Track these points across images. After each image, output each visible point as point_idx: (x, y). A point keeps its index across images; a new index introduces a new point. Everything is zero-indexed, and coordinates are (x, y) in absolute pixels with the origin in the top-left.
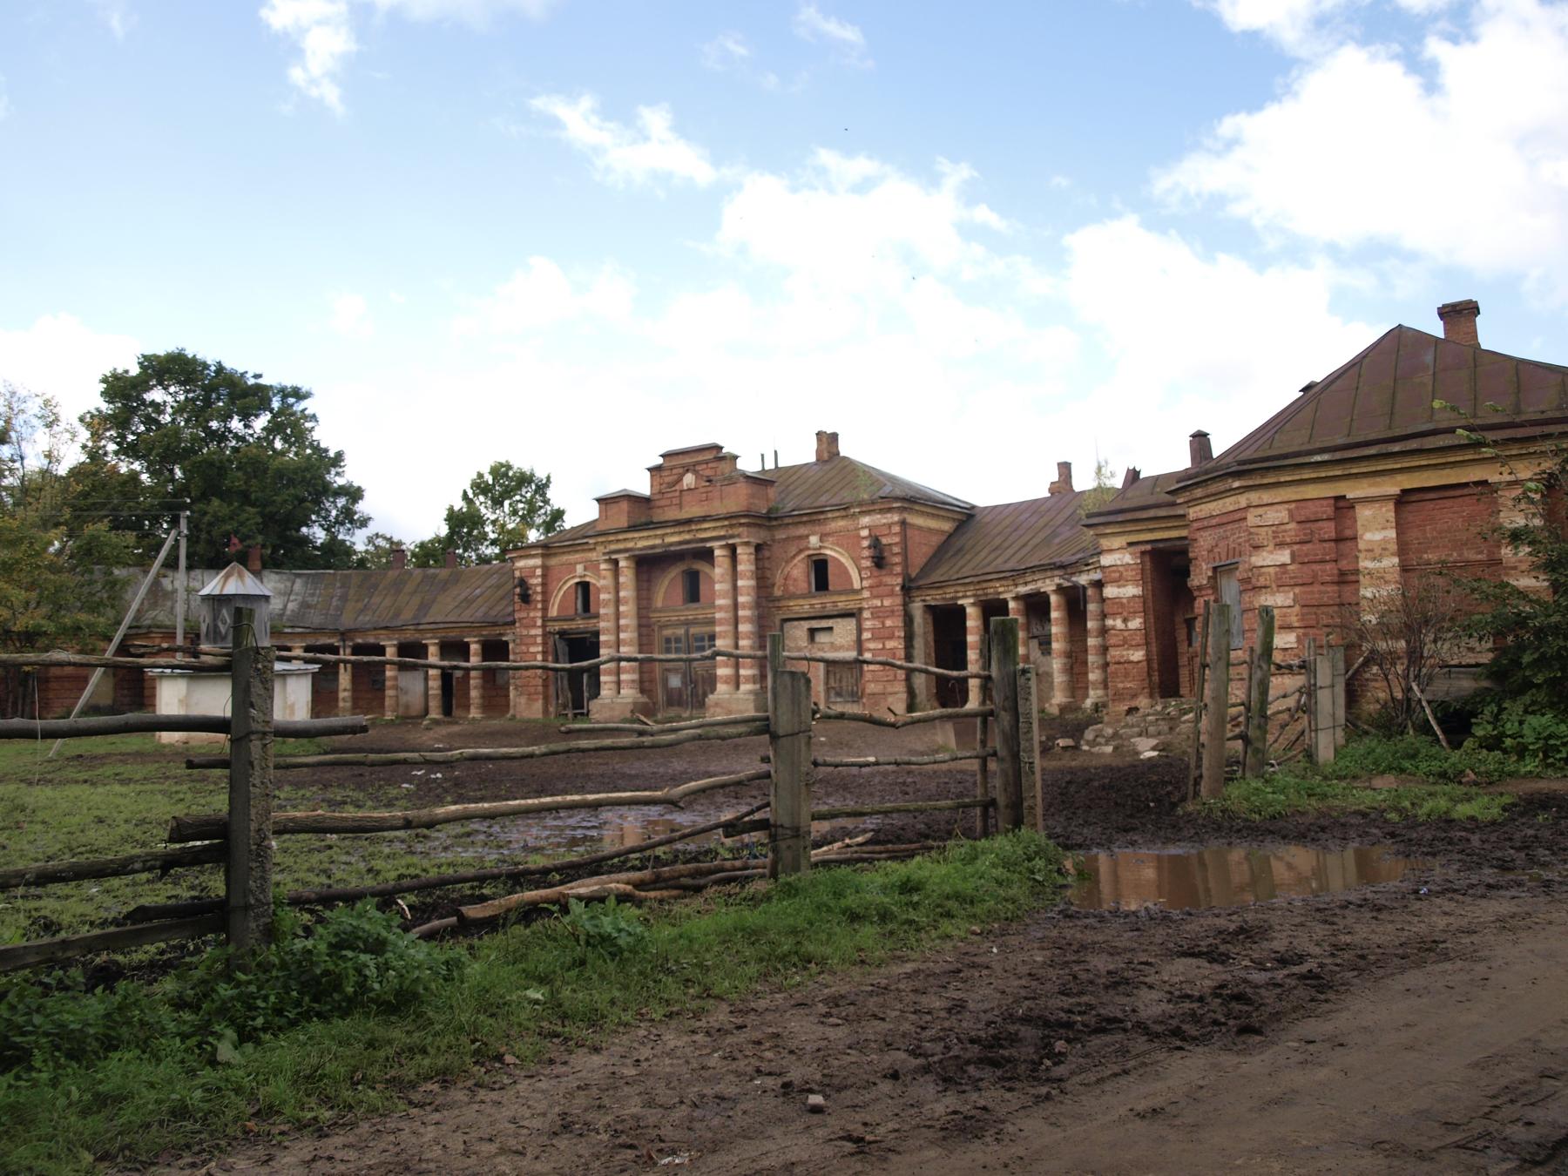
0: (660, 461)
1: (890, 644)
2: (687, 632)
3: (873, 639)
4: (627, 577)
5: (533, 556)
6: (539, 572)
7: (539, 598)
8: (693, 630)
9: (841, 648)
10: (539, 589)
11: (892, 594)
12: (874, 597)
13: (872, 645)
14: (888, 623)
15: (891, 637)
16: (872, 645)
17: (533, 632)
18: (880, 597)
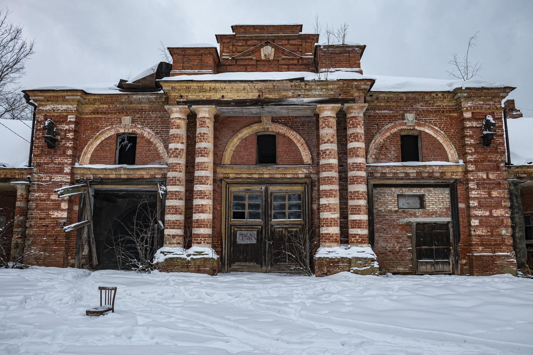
0: (230, 32)
1: (497, 213)
2: (267, 190)
3: (481, 206)
4: (206, 130)
5: (65, 101)
6: (71, 118)
7: (69, 144)
8: (272, 188)
9: (433, 214)
10: (70, 135)
11: (498, 168)
12: (478, 170)
13: (479, 213)
14: (495, 194)
15: (498, 206)
16: (479, 213)
17: (58, 178)
18: (487, 170)
